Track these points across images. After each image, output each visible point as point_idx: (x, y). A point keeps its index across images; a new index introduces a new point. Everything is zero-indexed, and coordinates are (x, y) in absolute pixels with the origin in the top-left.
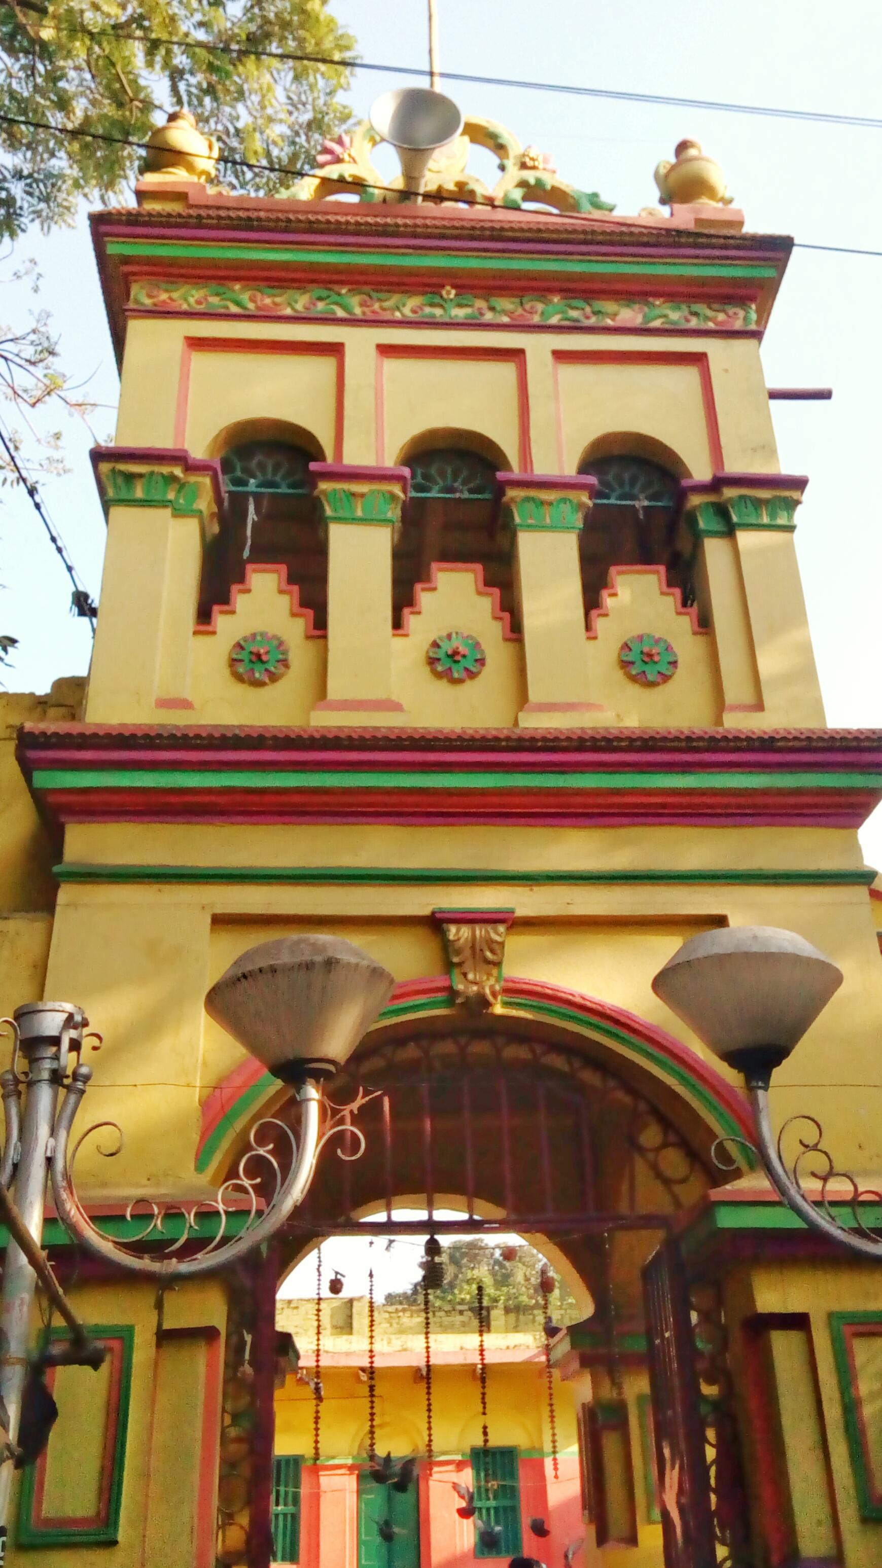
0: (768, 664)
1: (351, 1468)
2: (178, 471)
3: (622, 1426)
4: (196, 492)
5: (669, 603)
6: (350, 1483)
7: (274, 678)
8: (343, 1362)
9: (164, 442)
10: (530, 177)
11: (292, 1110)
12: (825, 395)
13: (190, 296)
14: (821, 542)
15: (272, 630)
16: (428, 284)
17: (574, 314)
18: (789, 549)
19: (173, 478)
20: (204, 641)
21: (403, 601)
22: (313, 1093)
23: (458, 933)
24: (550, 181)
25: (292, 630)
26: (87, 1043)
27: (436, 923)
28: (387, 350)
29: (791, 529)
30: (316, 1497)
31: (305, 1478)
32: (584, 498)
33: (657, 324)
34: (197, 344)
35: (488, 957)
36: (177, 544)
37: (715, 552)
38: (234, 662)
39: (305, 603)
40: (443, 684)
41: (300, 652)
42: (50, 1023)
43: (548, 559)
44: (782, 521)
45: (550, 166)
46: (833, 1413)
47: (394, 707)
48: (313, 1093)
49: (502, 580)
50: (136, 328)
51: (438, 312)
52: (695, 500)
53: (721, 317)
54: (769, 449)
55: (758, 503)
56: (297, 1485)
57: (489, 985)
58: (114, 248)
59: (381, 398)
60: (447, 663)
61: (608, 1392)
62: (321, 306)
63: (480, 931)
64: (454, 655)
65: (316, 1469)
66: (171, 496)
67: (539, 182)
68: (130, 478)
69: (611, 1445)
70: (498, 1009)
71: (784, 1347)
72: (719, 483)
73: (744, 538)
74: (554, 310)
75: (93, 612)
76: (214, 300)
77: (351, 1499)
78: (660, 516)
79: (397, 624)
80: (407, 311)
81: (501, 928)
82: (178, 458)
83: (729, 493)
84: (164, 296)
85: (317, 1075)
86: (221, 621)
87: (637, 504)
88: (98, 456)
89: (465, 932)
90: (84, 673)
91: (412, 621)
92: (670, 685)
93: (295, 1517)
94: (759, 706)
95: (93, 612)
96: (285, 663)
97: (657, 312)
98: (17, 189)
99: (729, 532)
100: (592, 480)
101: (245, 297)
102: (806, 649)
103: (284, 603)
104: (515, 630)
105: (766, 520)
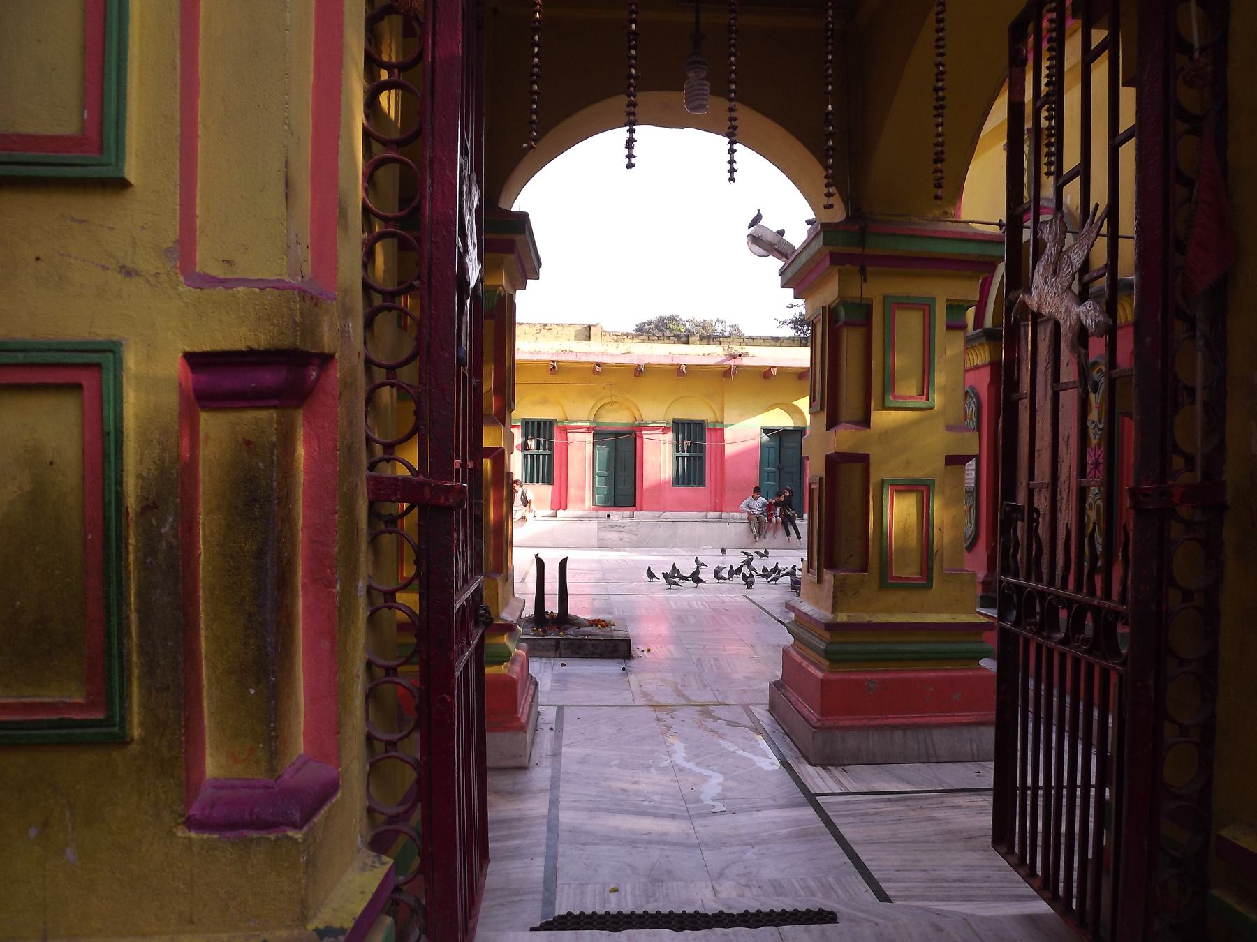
1: (589, 428)
3: (867, 323)
6: (589, 437)
8: (584, 359)
56: (552, 437)
61: (854, 292)
65: (565, 429)
69: (851, 342)
77: (589, 448)
93: (551, 457)
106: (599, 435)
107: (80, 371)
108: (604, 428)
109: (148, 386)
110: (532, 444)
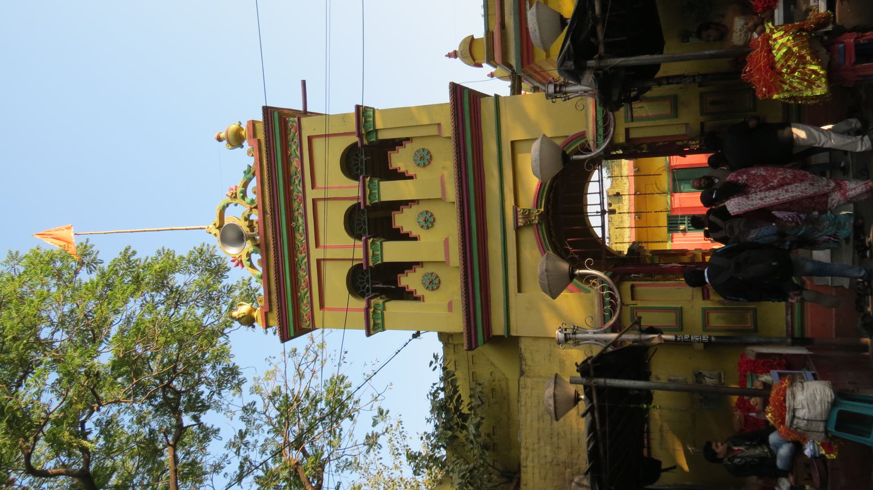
0: (426, 121)
1: (672, 196)
2: (371, 310)
5: (401, 150)
6: (677, 196)
7: (437, 277)
8: (633, 202)
9: (362, 315)
10: (240, 195)
11: (582, 276)
12: (304, 83)
13: (305, 309)
14: (380, 100)
15: (421, 278)
16: (291, 232)
17: (297, 182)
18: (384, 112)
19: (374, 312)
21: (406, 237)
22: (577, 272)
23: (521, 222)
24: (240, 189)
26: (564, 327)
27: (518, 229)
28: (317, 245)
29: (374, 110)
30: (682, 209)
31: (674, 214)
32: (368, 179)
33: (298, 153)
35: (527, 214)
36: (394, 308)
37: (383, 136)
38: (433, 289)
40: (436, 224)
41: (428, 269)
42: (560, 335)
43: (389, 191)
44: (371, 113)
45: (234, 187)
47: (446, 242)
48: (577, 272)
49: (397, 205)
51: (301, 228)
52: (365, 142)
53: (293, 130)
54: (344, 117)
56: (677, 216)
58: (292, 335)
60: (428, 223)
62: (303, 267)
64: (426, 221)
65: (672, 209)
66: (379, 312)
67: (241, 192)
68: (375, 324)
70: (542, 209)
71: (633, 135)
72: (360, 135)
74: (297, 189)
76: (305, 301)
77: (683, 195)
78: (371, 152)
79: (415, 239)
80: (302, 239)
81: (519, 209)
82: (367, 310)
84: (305, 317)
85: (573, 271)
87: (364, 159)
88: (369, 334)
89: (520, 220)
90: (436, 333)
91: (414, 234)
92: (431, 151)
94: (439, 124)
96: (432, 274)
97: (293, 153)
98: (219, 368)
99: (376, 131)
100: (361, 177)
101: (303, 291)
102: (418, 107)
103: (411, 275)
105: (371, 119)
106: (674, 190)
107: (706, 312)
108: (671, 187)
109: (708, 304)
110: (682, 227)
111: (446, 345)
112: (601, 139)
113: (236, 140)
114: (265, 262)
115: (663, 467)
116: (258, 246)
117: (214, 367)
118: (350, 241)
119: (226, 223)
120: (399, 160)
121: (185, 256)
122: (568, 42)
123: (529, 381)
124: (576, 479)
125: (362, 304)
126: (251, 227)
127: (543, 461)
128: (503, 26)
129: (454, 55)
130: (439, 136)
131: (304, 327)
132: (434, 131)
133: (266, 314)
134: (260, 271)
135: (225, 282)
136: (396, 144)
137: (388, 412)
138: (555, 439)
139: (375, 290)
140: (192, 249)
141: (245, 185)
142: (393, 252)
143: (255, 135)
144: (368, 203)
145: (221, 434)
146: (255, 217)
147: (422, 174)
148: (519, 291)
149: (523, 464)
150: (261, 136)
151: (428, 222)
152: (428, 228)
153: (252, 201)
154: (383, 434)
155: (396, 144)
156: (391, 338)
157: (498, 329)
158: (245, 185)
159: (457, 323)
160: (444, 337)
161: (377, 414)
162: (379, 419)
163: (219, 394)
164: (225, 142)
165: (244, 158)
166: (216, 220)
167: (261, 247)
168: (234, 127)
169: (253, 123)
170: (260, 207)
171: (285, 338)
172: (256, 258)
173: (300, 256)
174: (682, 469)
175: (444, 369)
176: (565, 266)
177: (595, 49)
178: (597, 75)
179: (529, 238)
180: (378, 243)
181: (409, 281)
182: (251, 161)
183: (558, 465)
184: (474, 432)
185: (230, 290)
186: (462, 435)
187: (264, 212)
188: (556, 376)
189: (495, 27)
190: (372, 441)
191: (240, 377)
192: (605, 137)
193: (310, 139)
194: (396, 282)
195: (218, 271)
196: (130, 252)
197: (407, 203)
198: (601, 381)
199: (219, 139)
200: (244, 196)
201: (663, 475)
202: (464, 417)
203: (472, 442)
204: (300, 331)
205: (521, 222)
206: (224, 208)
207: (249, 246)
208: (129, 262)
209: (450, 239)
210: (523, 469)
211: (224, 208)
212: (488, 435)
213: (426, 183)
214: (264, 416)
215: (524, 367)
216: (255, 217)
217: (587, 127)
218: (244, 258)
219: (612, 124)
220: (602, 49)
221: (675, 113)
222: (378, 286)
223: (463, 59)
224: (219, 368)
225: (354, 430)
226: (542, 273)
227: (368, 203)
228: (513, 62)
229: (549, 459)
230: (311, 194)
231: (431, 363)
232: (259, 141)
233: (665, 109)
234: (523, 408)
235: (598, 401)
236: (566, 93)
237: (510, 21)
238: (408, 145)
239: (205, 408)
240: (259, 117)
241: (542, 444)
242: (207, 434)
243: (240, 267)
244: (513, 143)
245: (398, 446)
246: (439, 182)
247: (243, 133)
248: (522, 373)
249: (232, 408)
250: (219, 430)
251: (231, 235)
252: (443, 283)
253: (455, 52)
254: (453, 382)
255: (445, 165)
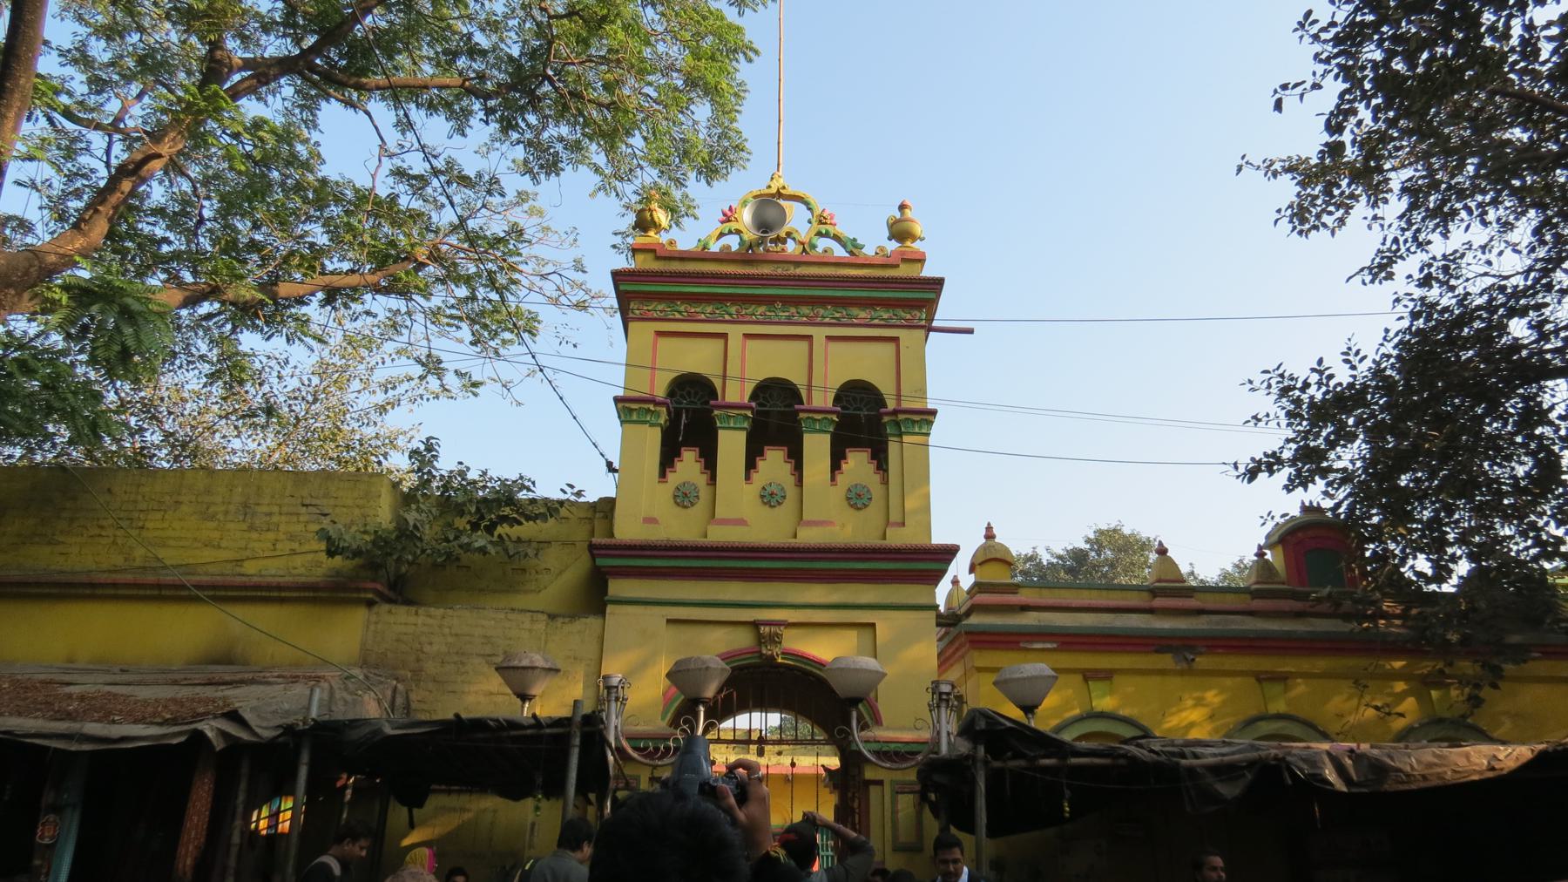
0: (909, 505)
2: (652, 407)
4: (658, 415)
5: (872, 467)
7: (693, 504)
10: (823, 229)
12: (970, 331)
16: (769, 301)
19: (649, 410)
20: (662, 486)
21: (751, 465)
22: (702, 709)
23: (765, 630)
25: (701, 480)
27: (755, 625)
28: (747, 336)
34: (659, 334)
35: (775, 639)
36: (652, 438)
38: (675, 497)
39: (706, 467)
41: (704, 491)
43: (817, 446)
46: (888, 814)
47: (741, 522)
49: (796, 457)
50: (632, 325)
52: (886, 419)
54: (922, 393)
55: (914, 422)
57: (777, 650)
59: (744, 359)
63: (773, 629)
64: (772, 494)
68: (631, 410)
71: (873, 790)
72: (895, 412)
73: (906, 438)
74: (827, 313)
75: (615, 471)
79: (748, 478)
83: (901, 417)
85: (703, 703)
86: (670, 476)
88: (617, 400)
91: (754, 476)
95: (615, 471)
99: (900, 435)
102: (927, 496)
104: (800, 482)
111: (593, 506)
112: (876, 747)
113: (900, 231)
114: (725, 257)
115: (416, 811)
116: (750, 247)
117: (561, 139)
118: (749, 388)
119: (781, 202)
120: (858, 463)
121: (735, 125)
122: (1008, 724)
123: (541, 626)
124: (400, 687)
125: (660, 392)
126: (778, 240)
127: (423, 639)
128: (1025, 608)
129: (990, 535)
130: (888, 523)
131: (632, 305)
132: (895, 516)
133: (653, 251)
134: (715, 247)
135: (692, 175)
136: (880, 458)
137: (475, 395)
138: (456, 658)
139: (678, 413)
140: (744, 136)
141: (837, 238)
142: (731, 444)
143: (905, 260)
144: (802, 415)
145: (457, 137)
146: (791, 247)
147: (837, 494)
148: (669, 621)
149: (422, 610)
150: (904, 271)
151: (770, 498)
152: (762, 497)
153: (814, 247)
154: (442, 386)
155: (880, 458)
156: (610, 432)
157: (617, 587)
158: (837, 238)
159: (627, 529)
160: (606, 507)
161: (474, 379)
162: (465, 381)
163: (519, 142)
164: (898, 215)
165: (874, 241)
166: (789, 191)
167: (747, 255)
168: (918, 229)
169: (920, 260)
170: (806, 258)
171: (618, 276)
172: (733, 243)
173: (733, 310)
174: (404, 836)
175: (561, 503)
176: (710, 692)
177: (995, 758)
178: (967, 757)
179: (742, 640)
180: (746, 425)
181: (689, 463)
182: (869, 251)
183: (418, 660)
184: (477, 545)
185: (680, 183)
186: (461, 523)
187: (798, 264)
188: (558, 671)
189: (1024, 597)
190: (432, 365)
191: (543, 176)
192: (877, 753)
193: (895, 340)
194: (689, 443)
195: (710, 172)
196: (751, 54)
197: (798, 468)
198: (577, 741)
199: (902, 207)
200: (819, 234)
201: (405, 810)
202: (490, 529)
203: (456, 538)
204: (625, 301)
205: (765, 630)
206: (807, 204)
207: (750, 235)
208: (735, 51)
209: (745, 529)
210: (413, 609)
211: (807, 204)
212: (458, 559)
213: (823, 500)
214: (479, 204)
215: (560, 620)
216: (791, 247)
217: (888, 728)
218: (733, 226)
219: (895, 766)
220: (997, 764)
221: (898, 848)
222: (683, 419)
223: (983, 548)
224: (559, 147)
225: (455, 347)
226: (704, 662)
227: (802, 415)
228: (974, 620)
229: (427, 648)
230: (819, 333)
231: (572, 487)
232: (897, 266)
233: (905, 836)
234: (502, 616)
235: (551, 735)
236: (938, 707)
237: (1030, 619)
238: (877, 478)
239: (507, 126)
240: (928, 272)
241: (450, 640)
242: (460, 120)
243: (721, 217)
244: (873, 625)
245: (401, 389)
246: (822, 519)
247: (908, 243)
248: (552, 617)
249: (494, 156)
250: (464, 135)
251: (769, 209)
252: (684, 511)
253: (993, 537)
254: (543, 517)
255: (848, 529)
